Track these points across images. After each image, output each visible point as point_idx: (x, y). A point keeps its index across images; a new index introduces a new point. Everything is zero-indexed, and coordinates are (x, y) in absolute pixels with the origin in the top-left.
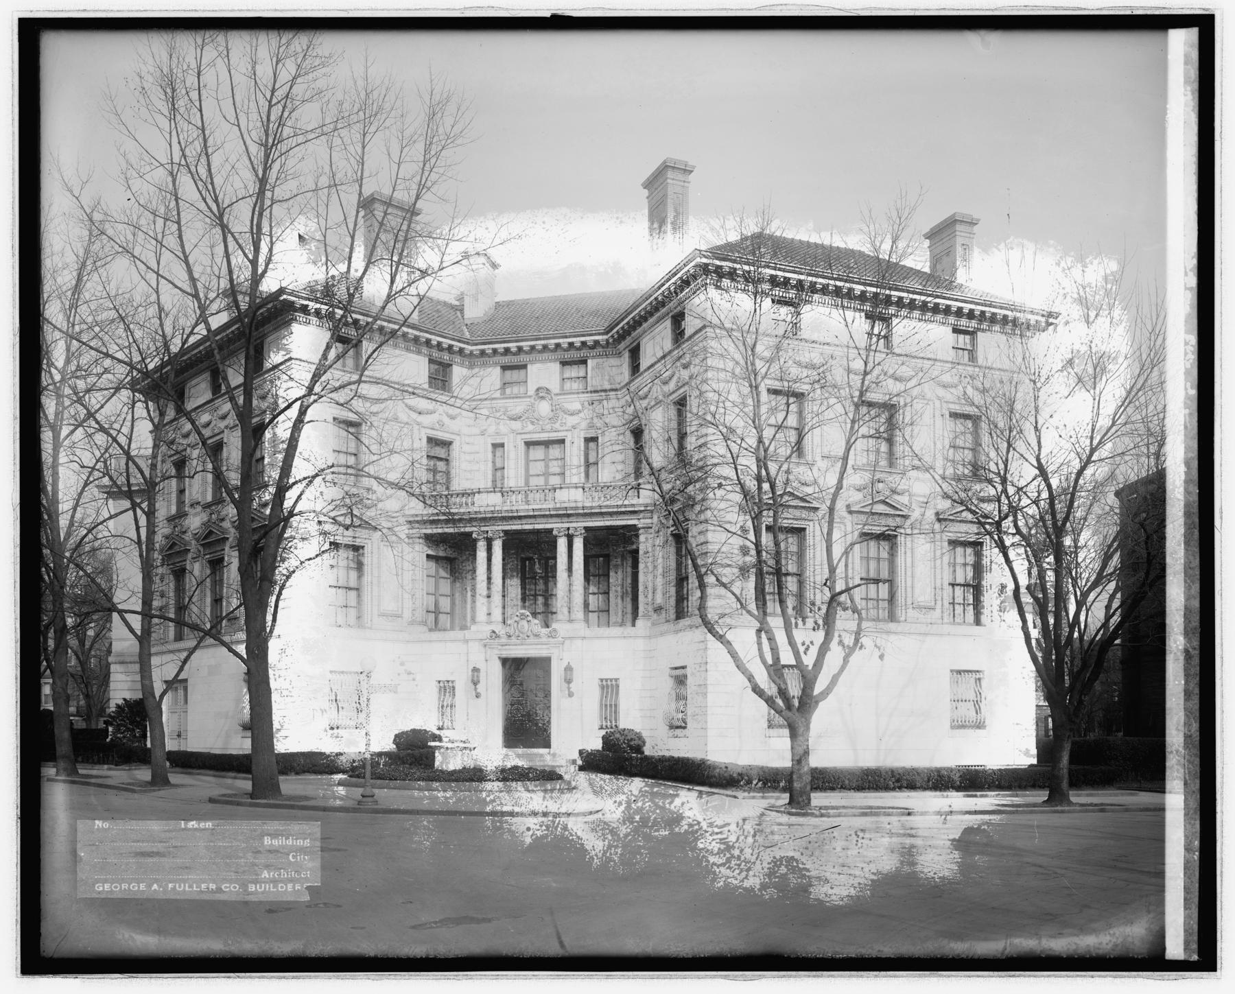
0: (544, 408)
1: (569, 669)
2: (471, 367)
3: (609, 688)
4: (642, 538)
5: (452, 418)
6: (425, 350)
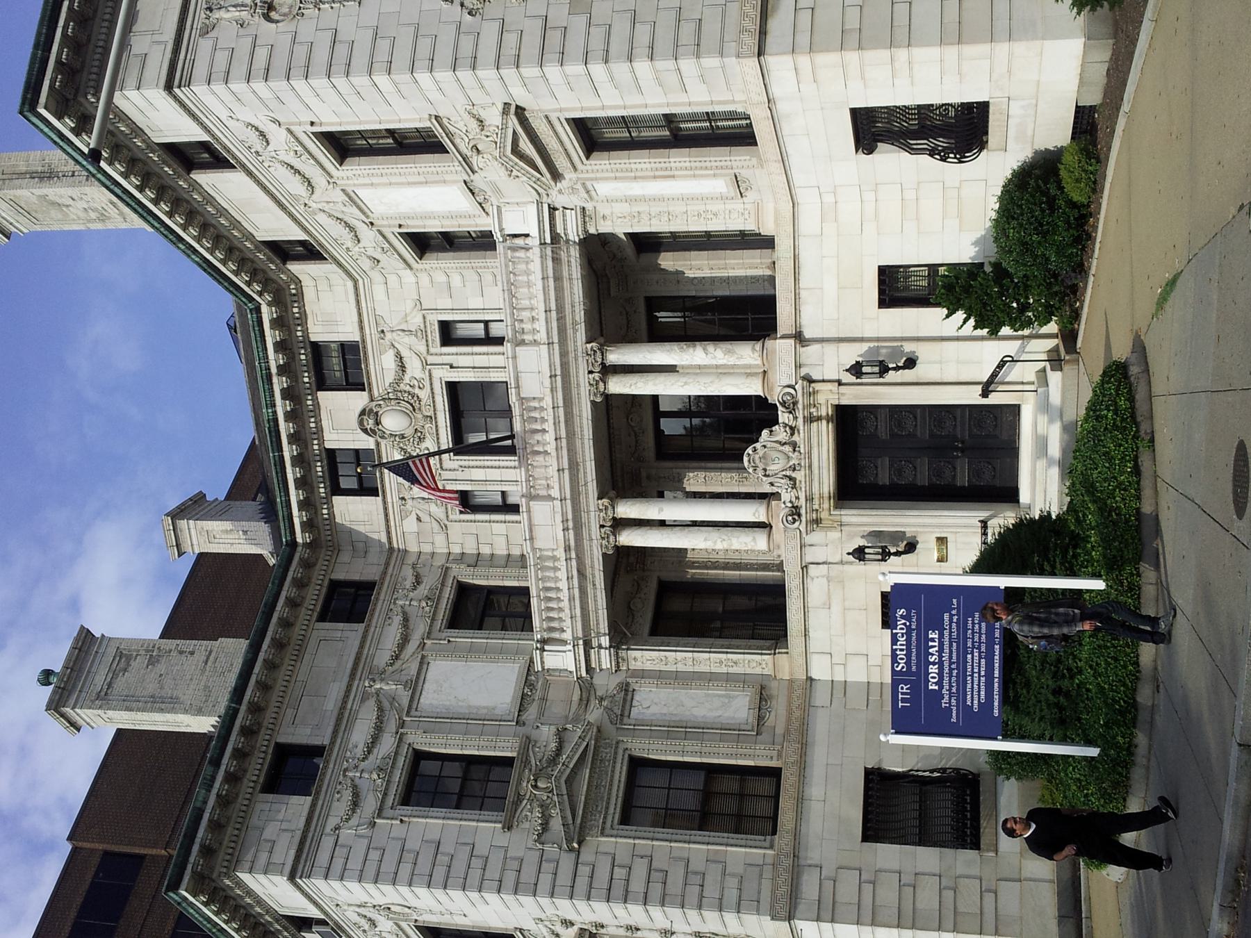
0: (393, 422)
1: (856, 369)
2: (336, 549)
3: (895, 287)
4: (605, 228)
5: (418, 580)
6: (297, 631)
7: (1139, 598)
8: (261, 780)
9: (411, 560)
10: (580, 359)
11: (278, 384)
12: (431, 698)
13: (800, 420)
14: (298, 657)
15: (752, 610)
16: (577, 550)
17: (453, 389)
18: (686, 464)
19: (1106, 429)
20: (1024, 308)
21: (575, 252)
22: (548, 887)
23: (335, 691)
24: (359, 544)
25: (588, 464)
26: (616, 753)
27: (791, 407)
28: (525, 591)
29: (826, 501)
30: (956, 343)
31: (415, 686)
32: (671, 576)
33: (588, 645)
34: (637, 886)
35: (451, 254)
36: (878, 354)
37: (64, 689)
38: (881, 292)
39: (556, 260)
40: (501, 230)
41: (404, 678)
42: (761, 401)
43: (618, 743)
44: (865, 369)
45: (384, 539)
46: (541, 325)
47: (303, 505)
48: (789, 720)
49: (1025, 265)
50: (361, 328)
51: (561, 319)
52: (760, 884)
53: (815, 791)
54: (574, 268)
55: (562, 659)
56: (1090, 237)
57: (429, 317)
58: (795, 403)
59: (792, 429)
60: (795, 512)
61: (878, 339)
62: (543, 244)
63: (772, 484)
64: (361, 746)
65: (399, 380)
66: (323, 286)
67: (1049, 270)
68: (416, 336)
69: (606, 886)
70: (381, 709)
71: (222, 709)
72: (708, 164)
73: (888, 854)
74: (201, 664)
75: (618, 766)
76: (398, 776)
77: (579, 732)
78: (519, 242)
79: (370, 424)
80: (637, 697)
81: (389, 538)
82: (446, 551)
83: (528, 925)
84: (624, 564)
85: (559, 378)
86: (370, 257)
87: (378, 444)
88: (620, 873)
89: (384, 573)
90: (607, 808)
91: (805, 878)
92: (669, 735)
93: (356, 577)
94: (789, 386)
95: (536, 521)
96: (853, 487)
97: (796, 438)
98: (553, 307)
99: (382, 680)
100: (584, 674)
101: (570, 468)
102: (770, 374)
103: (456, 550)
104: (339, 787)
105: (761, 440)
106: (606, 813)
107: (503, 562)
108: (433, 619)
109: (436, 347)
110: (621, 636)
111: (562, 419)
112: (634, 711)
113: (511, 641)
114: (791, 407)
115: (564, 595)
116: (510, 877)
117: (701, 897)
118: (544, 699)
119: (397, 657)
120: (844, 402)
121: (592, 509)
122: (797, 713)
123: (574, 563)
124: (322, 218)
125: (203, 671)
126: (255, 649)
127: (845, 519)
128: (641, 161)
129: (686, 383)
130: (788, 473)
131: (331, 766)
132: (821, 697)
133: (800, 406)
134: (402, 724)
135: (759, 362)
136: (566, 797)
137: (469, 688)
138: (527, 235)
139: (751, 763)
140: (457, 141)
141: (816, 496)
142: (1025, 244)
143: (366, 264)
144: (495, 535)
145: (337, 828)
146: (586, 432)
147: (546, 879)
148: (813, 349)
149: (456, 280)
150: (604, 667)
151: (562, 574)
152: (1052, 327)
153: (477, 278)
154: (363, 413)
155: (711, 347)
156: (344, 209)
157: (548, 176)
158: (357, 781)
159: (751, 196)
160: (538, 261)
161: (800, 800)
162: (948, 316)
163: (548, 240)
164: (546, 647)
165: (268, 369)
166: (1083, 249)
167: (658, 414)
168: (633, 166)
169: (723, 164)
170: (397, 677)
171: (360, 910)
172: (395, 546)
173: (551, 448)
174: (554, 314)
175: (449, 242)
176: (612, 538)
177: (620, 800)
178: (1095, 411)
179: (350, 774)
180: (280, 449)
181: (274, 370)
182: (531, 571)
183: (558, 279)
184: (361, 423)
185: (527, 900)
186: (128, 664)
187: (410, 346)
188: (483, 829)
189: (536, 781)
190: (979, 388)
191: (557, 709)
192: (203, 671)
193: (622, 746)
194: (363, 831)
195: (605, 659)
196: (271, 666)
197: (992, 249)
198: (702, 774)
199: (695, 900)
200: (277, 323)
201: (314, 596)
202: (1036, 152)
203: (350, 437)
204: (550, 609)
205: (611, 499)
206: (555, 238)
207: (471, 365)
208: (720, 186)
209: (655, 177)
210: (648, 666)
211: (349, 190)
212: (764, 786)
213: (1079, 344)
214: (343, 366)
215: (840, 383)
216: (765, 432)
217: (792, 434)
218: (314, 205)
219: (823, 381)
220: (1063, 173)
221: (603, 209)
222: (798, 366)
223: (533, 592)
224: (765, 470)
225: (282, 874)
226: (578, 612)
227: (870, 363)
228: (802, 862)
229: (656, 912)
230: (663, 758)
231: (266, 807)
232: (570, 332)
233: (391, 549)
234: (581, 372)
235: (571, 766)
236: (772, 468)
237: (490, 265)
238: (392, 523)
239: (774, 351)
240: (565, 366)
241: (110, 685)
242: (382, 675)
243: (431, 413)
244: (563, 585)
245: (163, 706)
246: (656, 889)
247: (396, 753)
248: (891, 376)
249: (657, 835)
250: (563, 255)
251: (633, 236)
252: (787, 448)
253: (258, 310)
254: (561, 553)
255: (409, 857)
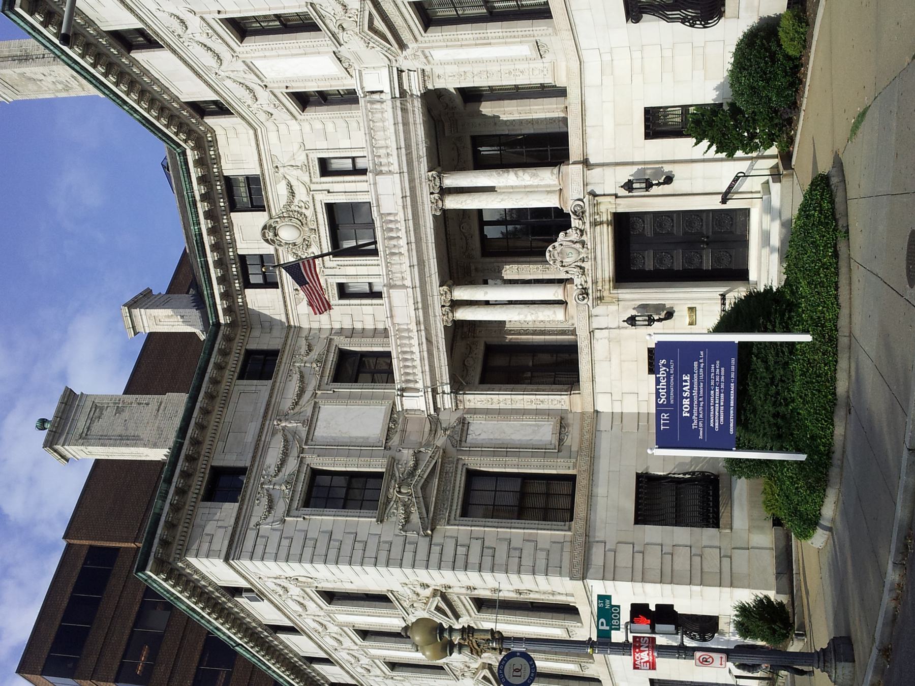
0: (287, 234)
1: (629, 186)
3: (657, 124)
4: (439, 84)
5: (310, 348)
6: (223, 386)
7: (836, 346)
8: (202, 492)
9: (304, 334)
10: (424, 184)
11: (202, 207)
12: (322, 431)
13: (588, 225)
14: (225, 404)
15: (554, 363)
16: (425, 324)
17: (330, 208)
18: (504, 259)
19: (813, 224)
20: (752, 136)
21: (418, 103)
22: (410, 562)
23: (253, 428)
24: (266, 323)
25: (432, 261)
26: (457, 467)
27: (581, 215)
28: (388, 355)
29: (607, 283)
30: (702, 164)
31: (311, 423)
32: (494, 341)
33: (434, 392)
34: (474, 559)
35: (325, 108)
36: (645, 174)
37: (55, 432)
38: (647, 127)
39: (404, 110)
40: (362, 88)
41: (302, 418)
42: (558, 212)
43: (458, 460)
44: (635, 186)
45: (284, 319)
46: (394, 160)
47: (224, 296)
48: (581, 442)
49: (754, 104)
50: (261, 165)
51: (409, 154)
52: (561, 555)
53: (601, 490)
54: (417, 116)
55: (416, 403)
56: (801, 82)
57: (311, 156)
58: (583, 213)
59: (582, 231)
60: (584, 292)
61: (645, 163)
62: (394, 98)
63: (567, 272)
64: (273, 467)
65: (290, 203)
66: (231, 134)
67: (771, 108)
68: (302, 169)
69: (452, 559)
70: (286, 441)
71: (171, 443)
72: (516, 34)
73: (653, 533)
74: (155, 412)
75: (459, 476)
76: (301, 487)
77: (430, 453)
78: (376, 97)
79: (270, 236)
80: (471, 428)
81: (288, 318)
82: (329, 327)
83: (397, 587)
84: (460, 335)
85: (408, 199)
86: (265, 112)
87: (276, 250)
88: (461, 550)
89: (285, 344)
90: (451, 506)
91: (594, 550)
92: (494, 454)
93: (265, 347)
94: (579, 200)
95: (394, 303)
96: (627, 273)
97: (584, 238)
98: (403, 145)
99: (286, 420)
100: (432, 412)
101: (418, 264)
102: (564, 191)
103: (337, 326)
105: (559, 240)
106: (451, 509)
107: (371, 334)
108: (322, 376)
109: (317, 177)
110: (459, 385)
111: (412, 229)
112: (470, 437)
113: (379, 390)
114: (581, 215)
115: (417, 356)
116: (383, 555)
117: (520, 565)
118: (404, 431)
119: (297, 403)
120: (620, 210)
121: (435, 294)
122: (587, 436)
123: (423, 333)
124: (228, 83)
125: (156, 416)
126: (193, 400)
127: (621, 296)
128: (465, 33)
129: (502, 200)
130: (579, 264)
131: (252, 481)
132: (604, 424)
133: (587, 214)
134: (302, 451)
135: (556, 182)
136: (421, 499)
137: (350, 423)
138: (382, 92)
139: (554, 472)
140: (328, 21)
141: (600, 280)
142: (752, 88)
143: (262, 117)
144: (364, 315)
146: (429, 238)
147: (408, 556)
148: (597, 171)
149: (330, 127)
150: (447, 407)
151: (415, 342)
152: (774, 150)
153: (345, 125)
154: (265, 228)
155: (520, 172)
156: (245, 76)
157: (396, 46)
158: (271, 492)
159: (548, 57)
160: (390, 110)
161: (590, 497)
162: (696, 144)
163: (398, 95)
164: (405, 394)
166: (796, 91)
167: (483, 224)
168: (460, 37)
169: (527, 33)
170: (297, 418)
171: (278, 581)
172: (292, 324)
173: (404, 250)
174: (403, 150)
175: (324, 98)
176: (450, 315)
177: (460, 500)
178: (805, 212)
179: (266, 487)
180: (205, 256)
181: (198, 198)
182: (392, 340)
183: (406, 124)
184: (264, 235)
185: (396, 571)
186: (101, 414)
187: (299, 178)
188: (363, 523)
189: (399, 488)
190: (720, 197)
191: (414, 437)
192: (156, 416)
193: (461, 462)
194: (277, 526)
195: (447, 401)
196: (206, 412)
197: (729, 93)
198: (519, 480)
199: (516, 568)
200: (199, 163)
201: (235, 361)
202: (761, 19)
203: (256, 246)
204: (406, 367)
205: (449, 286)
206: (403, 93)
207: (343, 190)
208: (525, 50)
209: (476, 45)
210: (479, 406)
211: (248, 61)
212: (565, 488)
213: (793, 163)
214: (248, 194)
215: (616, 196)
216: (562, 234)
217: (582, 235)
218: (222, 74)
219: (604, 195)
220: (781, 34)
221: (438, 70)
222: (585, 185)
223: (394, 355)
224: (562, 262)
225: (219, 557)
226: (427, 368)
227: (639, 181)
228: (591, 540)
229: (487, 576)
230: (491, 470)
231: (207, 511)
232: (415, 163)
233: (289, 326)
234: (425, 193)
235: (425, 477)
236: (567, 261)
237: (354, 115)
238: (289, 308)
239: (567, 174)
240: (413, 189)
241: (88, 429)
242: (286, 417)
243: (315, 227)
244: (416, 349)
245: (128, 442)
246: (487, 560)
247: (299, 471)
248: (655, 190)
249: (488, 524)
250: (409, 106)
251: (461, 91)
252: (578, 246)
253: (184, 153)
254: (413, 327)
255: (310, 543)
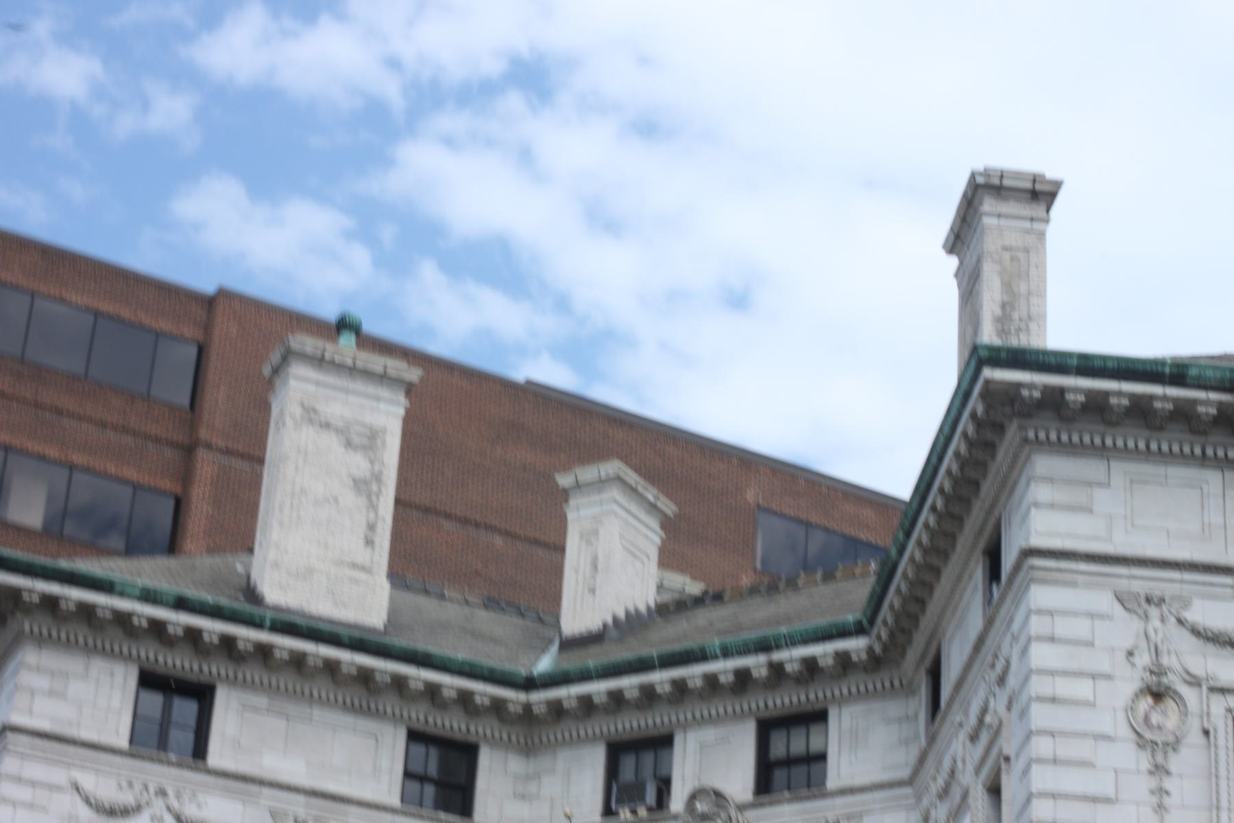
2: (528, 750)
6: (390, 703)
11: (756, 663)
79: (700, 807)
104: (138, 787)
125: (340, 563)
145: (77, 788)
154: (718, 794)
165: (778, 647)
181: (777, 656)
192: (340, 563)
200: (844, 660)
231: (119, 678)
241: (326, 426)
